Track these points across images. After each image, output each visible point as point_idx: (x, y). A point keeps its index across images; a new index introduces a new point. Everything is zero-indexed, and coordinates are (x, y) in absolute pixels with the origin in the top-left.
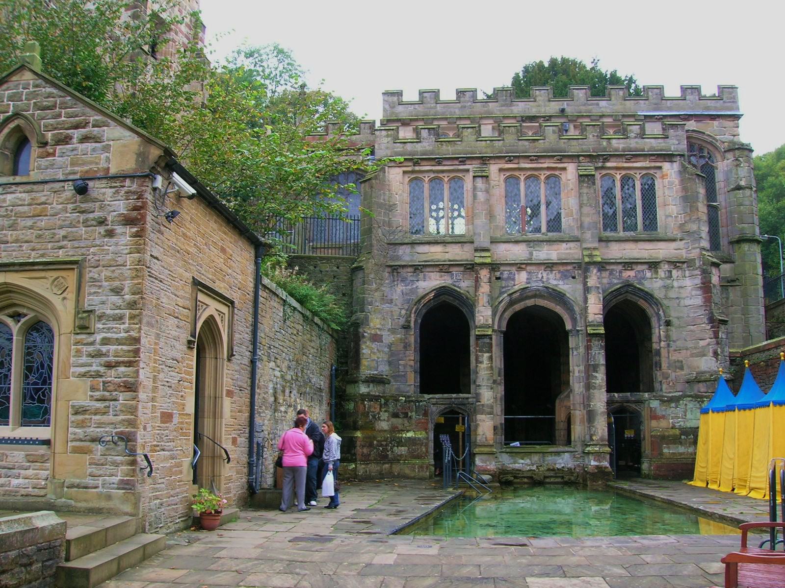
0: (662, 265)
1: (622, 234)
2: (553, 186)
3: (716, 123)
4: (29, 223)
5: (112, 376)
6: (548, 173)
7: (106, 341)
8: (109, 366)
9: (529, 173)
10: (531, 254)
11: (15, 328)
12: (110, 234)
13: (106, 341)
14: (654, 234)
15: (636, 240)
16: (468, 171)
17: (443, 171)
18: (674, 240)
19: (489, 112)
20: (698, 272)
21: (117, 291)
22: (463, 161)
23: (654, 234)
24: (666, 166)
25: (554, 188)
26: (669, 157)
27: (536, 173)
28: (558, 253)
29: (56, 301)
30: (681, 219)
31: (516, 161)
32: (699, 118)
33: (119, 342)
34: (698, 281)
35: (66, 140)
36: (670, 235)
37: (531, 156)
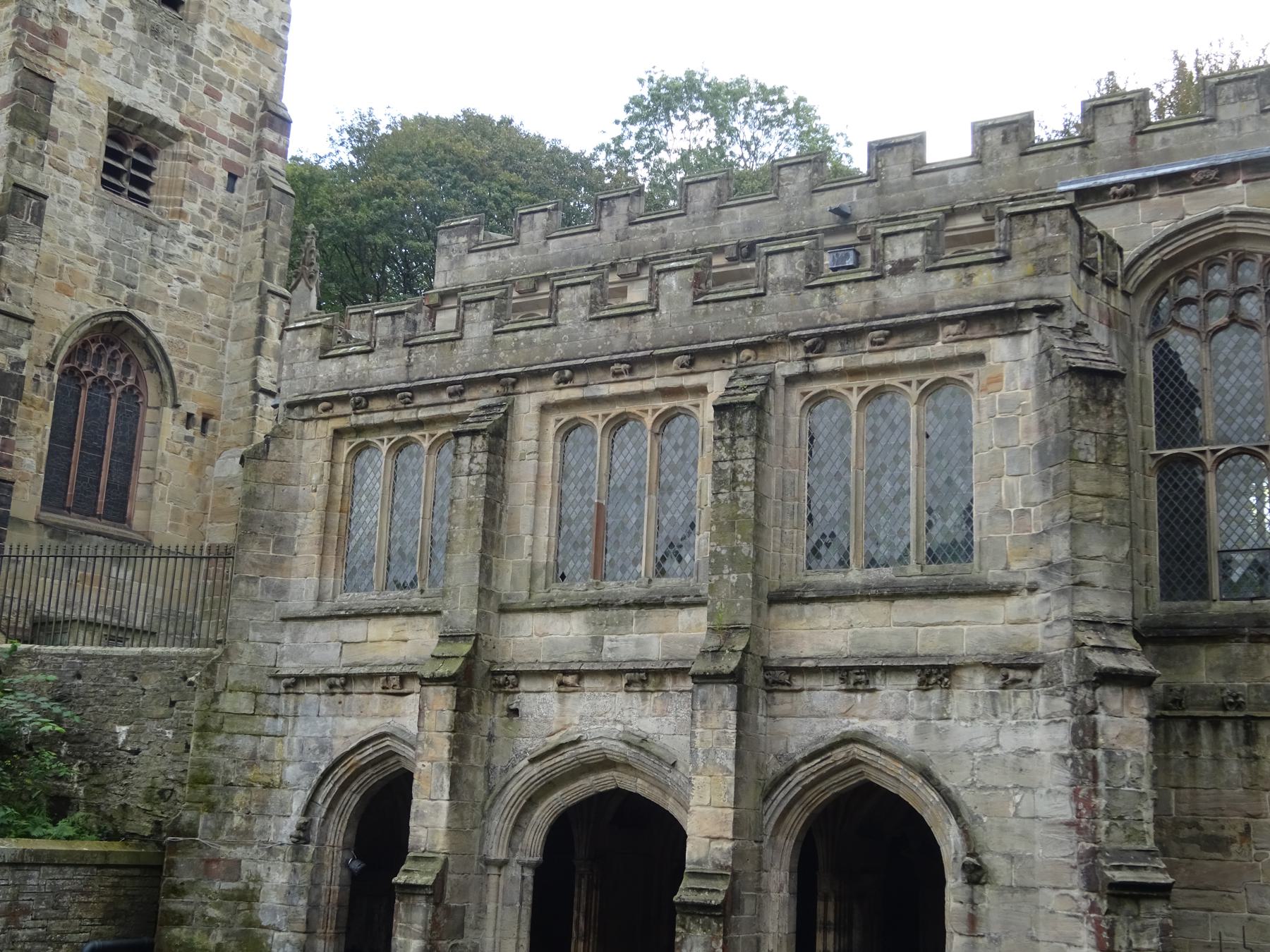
0: (965, 674)
1: (855, 576)
2: (681, 441)
6: (664, 405)
9: (617, 409)
10: (597, 642)
14: (953, 571)
15: (893, 594)
18: (1004, 591)
20: (1062, 704)
23: (953, 571)
25: (685, 446)
27: (633, 408)
28: (666, 641)
30: (1036, 522)
31: (580, 379)
34: (1062, 735)
36: (993, 574)
37: (612, 363)
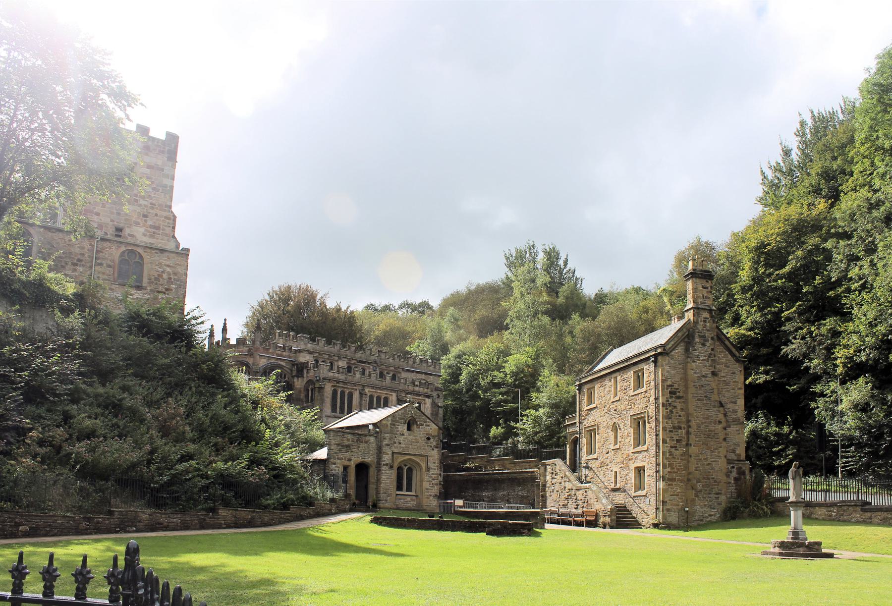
3: (432, 377)
4: (415, 444)
5: (433, 482)
7: (433, 474)
8: (433, 480)
11: (405, 469)
12: (433, 450)
13: (433, 474)
16: (356, 389)
17: (346, 388)
19: (346, 355)
21: (434, 463)
22: (355, 385)
24: (427, 400)
26: (428, 397)
29: (422, 464)
32: (426, 374)
33: (435, 474)
35: (422, 425)
